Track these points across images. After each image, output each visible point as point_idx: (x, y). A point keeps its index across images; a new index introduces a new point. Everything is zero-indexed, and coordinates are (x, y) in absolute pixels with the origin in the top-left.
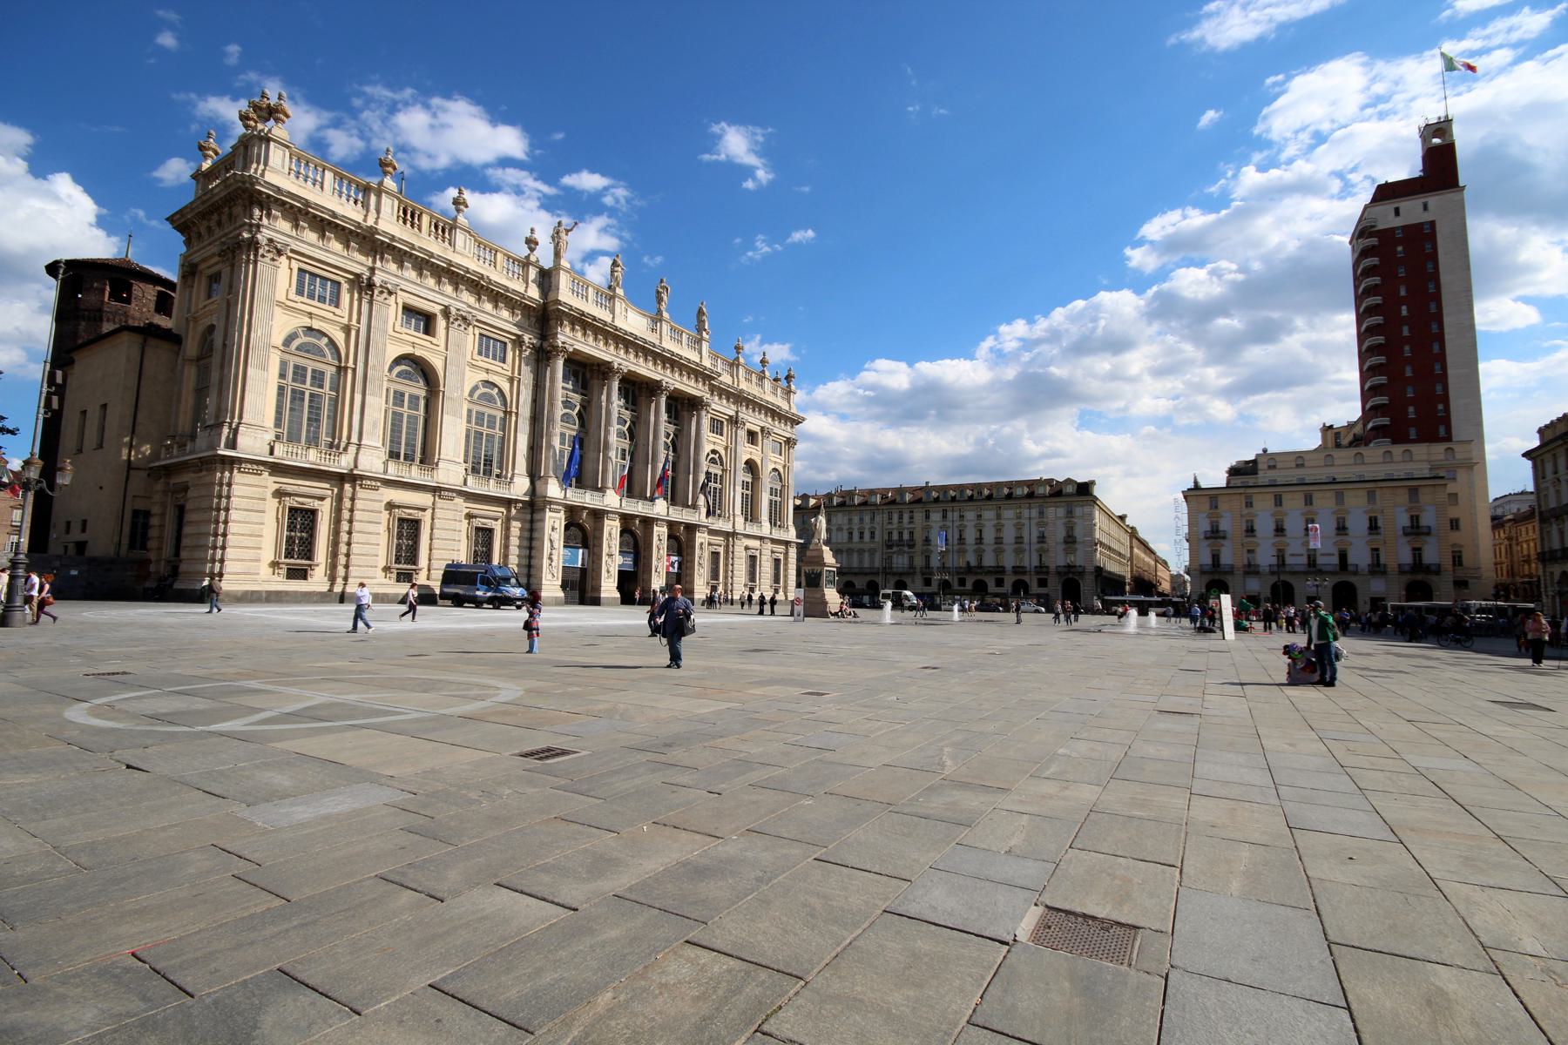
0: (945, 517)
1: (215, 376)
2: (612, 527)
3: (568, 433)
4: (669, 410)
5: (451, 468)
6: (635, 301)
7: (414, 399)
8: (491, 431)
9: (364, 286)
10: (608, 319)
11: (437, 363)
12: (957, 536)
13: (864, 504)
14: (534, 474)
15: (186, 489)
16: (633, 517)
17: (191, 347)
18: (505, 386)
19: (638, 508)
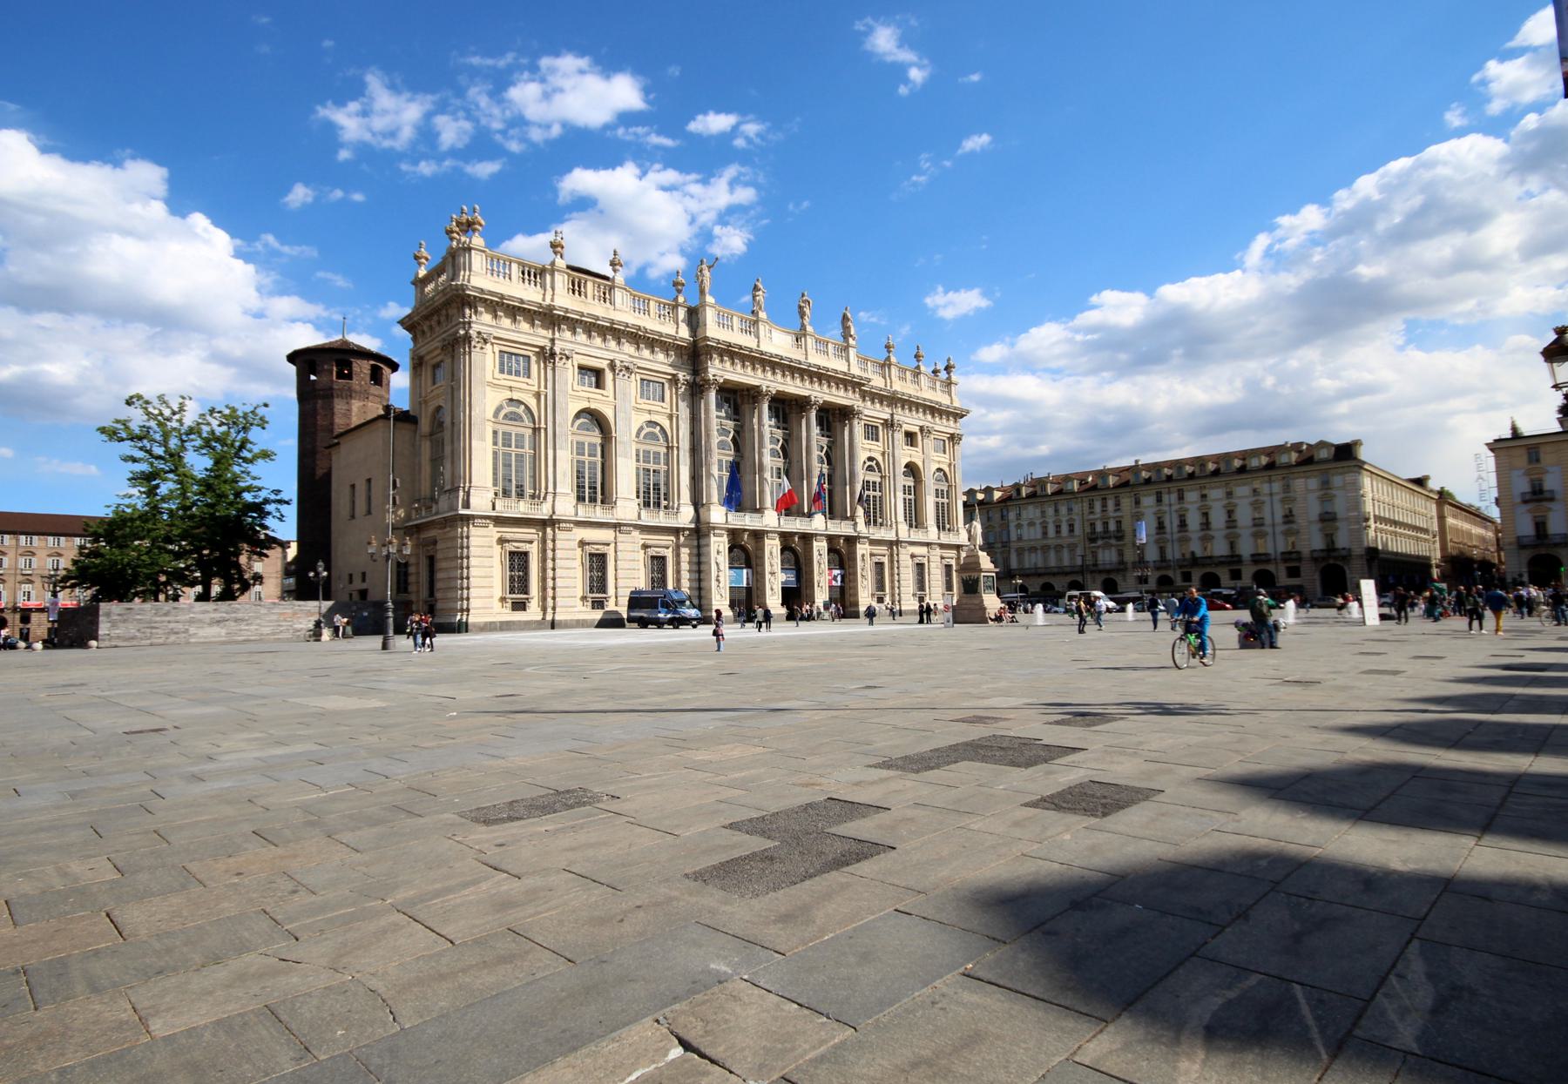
0: (1159, 500)
1: (448, 449)
2: (772, 546)
3: (725, 459)
4: (820, 422)
5: (627, 507)
6: (777, 321)
7: (592, 446)
8: (656, 467)
9: (547, 356)
10: (754, 346)
11: (608, 412)
12: (1176, 522)
13: (1059, 492)
14: (697, 503)
15: (435, 542)
16: (792, 534)
17: (425, 425)
18: (666, 423)
19: (796, 525)
